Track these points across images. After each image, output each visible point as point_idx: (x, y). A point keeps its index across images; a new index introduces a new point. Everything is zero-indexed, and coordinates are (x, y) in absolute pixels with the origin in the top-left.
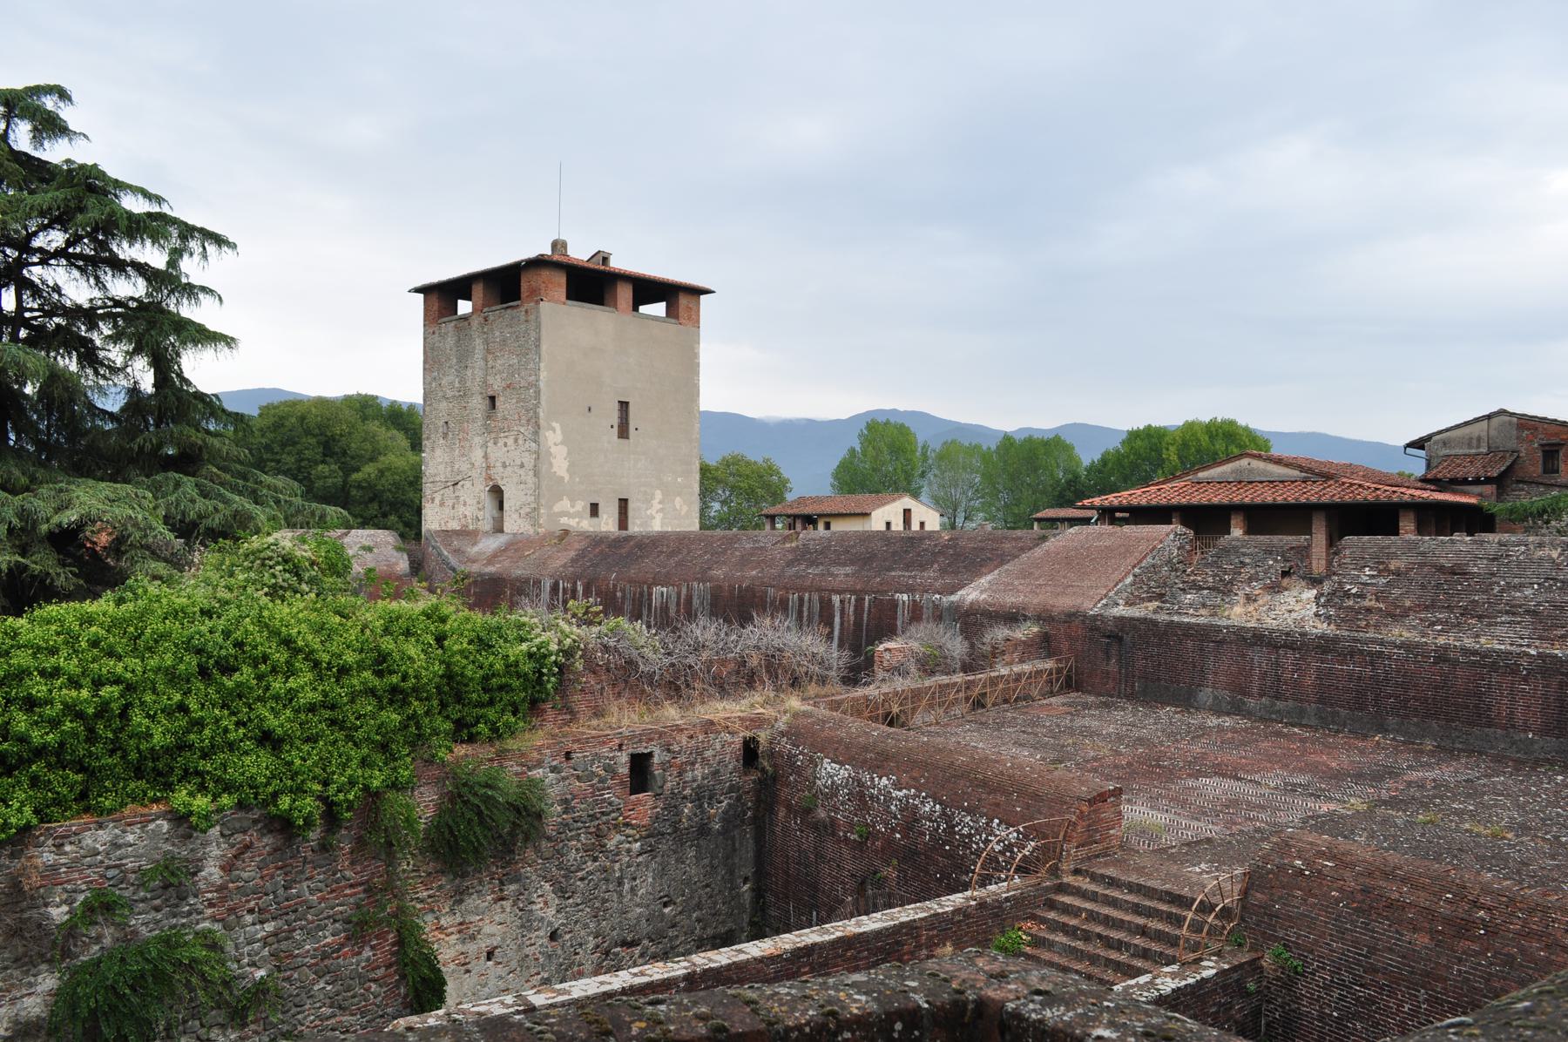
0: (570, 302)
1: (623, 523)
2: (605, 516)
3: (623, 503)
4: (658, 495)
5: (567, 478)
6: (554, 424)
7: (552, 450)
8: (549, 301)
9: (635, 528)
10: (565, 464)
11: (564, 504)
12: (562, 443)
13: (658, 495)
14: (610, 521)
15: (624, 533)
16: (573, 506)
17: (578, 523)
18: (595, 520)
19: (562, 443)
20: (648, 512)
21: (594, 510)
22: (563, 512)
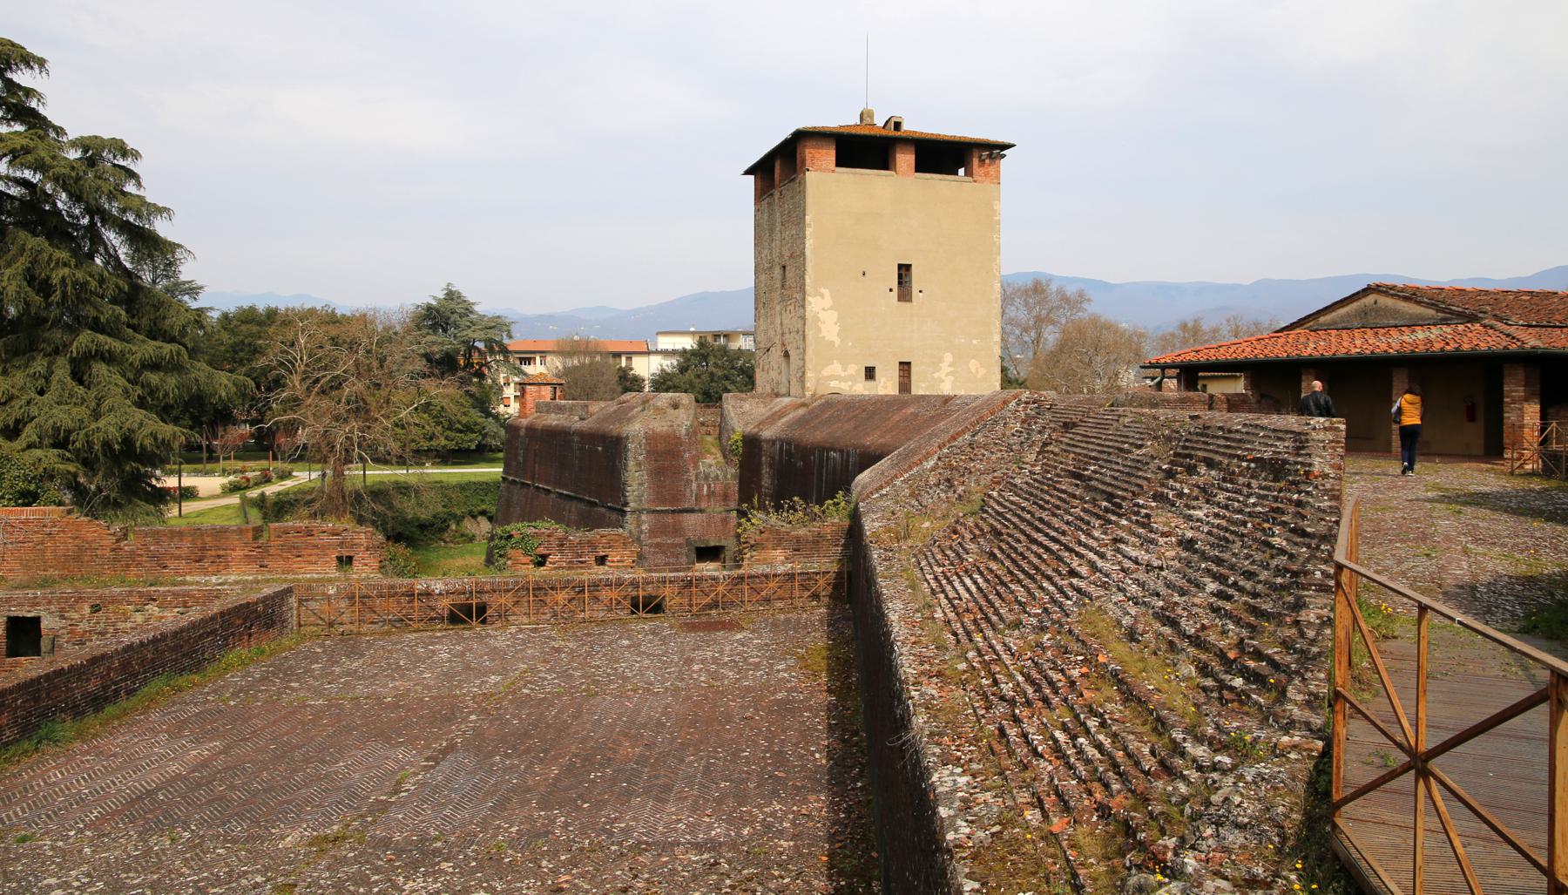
0: (919, 175)
1: (905, 386)
2: (883, 380)
3: (905, 367)
4: (948, 357)
5: (837, 341)
6: (822, 290)
7: (820, 315)
8: (816, 170)
9: (919, 388)
10: (837, 329)
11: (836, 368)
12: (831, 308)
13: (948, 357)
14: (889, 384)
15: (906, 396)
16: (845, 370)
17: (851, 387)
18: (870, 383)
19: (831, 308)
20: (936, 375)
21: (870, 373)
22: (831, 376)
